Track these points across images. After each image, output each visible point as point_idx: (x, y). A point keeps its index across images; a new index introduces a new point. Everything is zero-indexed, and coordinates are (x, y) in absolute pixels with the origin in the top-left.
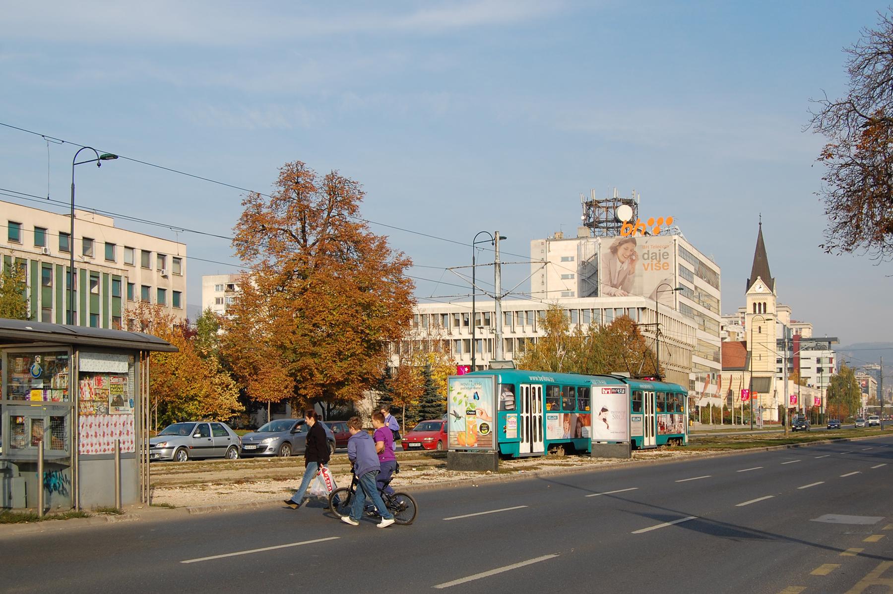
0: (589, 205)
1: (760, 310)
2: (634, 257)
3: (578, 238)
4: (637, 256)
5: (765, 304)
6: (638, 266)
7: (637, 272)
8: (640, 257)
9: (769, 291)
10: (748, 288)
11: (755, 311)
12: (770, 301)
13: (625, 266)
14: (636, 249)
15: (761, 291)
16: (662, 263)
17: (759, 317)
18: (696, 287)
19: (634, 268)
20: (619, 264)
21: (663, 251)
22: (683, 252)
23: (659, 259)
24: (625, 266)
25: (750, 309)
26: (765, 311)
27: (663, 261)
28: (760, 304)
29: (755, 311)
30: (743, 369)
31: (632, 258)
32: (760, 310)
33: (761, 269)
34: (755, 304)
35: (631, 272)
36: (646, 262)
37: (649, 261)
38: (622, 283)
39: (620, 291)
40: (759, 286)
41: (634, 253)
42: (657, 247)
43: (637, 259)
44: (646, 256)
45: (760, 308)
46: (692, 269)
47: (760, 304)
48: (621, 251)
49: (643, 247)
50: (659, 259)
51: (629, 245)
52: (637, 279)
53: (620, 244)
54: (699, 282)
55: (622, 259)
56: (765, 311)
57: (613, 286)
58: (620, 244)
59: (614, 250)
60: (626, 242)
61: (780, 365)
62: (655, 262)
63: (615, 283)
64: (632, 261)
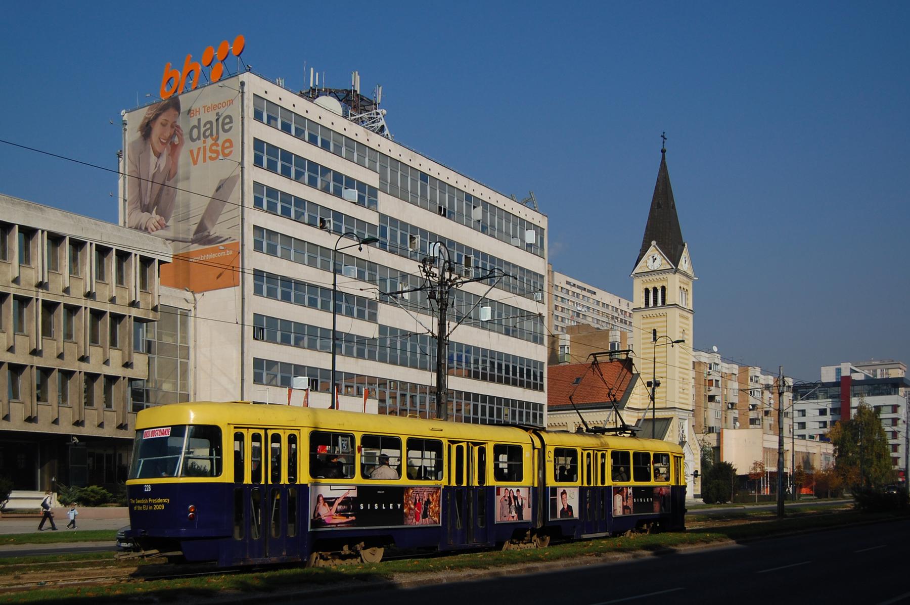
5: (663, 289)
6: (183, 157)
7: (180, 172)
8: (186, 137)
11: (647, 303)
14: (180, 122)
15: (656, 266)
16: (220, 142)
18: (383, 217)
19: (175, 164)
20: (153, 158)
27: (223, 137)
28: (655, 290)
29: (647, 303)
34: (647, 291)
35: (171, 173)
36: (195, 146)
37: (199, 143)
38: (157, 203)
39: (155, 217)
40: (654, 259)
41: (176, 130)
42: (215, 107)
44: (195, 131)
45: (656, 297)
46: (371, 179)
47: (655, 290)
48: (157, 130)
51: (171, 111)
53: (156, 117)
54: (389, 205)
55: (158, 149)
57: (146, 209)
60: (164, 109)
61: (823, 418)
62: (210, 141)
63: (147, 200)
64: (174, 148)
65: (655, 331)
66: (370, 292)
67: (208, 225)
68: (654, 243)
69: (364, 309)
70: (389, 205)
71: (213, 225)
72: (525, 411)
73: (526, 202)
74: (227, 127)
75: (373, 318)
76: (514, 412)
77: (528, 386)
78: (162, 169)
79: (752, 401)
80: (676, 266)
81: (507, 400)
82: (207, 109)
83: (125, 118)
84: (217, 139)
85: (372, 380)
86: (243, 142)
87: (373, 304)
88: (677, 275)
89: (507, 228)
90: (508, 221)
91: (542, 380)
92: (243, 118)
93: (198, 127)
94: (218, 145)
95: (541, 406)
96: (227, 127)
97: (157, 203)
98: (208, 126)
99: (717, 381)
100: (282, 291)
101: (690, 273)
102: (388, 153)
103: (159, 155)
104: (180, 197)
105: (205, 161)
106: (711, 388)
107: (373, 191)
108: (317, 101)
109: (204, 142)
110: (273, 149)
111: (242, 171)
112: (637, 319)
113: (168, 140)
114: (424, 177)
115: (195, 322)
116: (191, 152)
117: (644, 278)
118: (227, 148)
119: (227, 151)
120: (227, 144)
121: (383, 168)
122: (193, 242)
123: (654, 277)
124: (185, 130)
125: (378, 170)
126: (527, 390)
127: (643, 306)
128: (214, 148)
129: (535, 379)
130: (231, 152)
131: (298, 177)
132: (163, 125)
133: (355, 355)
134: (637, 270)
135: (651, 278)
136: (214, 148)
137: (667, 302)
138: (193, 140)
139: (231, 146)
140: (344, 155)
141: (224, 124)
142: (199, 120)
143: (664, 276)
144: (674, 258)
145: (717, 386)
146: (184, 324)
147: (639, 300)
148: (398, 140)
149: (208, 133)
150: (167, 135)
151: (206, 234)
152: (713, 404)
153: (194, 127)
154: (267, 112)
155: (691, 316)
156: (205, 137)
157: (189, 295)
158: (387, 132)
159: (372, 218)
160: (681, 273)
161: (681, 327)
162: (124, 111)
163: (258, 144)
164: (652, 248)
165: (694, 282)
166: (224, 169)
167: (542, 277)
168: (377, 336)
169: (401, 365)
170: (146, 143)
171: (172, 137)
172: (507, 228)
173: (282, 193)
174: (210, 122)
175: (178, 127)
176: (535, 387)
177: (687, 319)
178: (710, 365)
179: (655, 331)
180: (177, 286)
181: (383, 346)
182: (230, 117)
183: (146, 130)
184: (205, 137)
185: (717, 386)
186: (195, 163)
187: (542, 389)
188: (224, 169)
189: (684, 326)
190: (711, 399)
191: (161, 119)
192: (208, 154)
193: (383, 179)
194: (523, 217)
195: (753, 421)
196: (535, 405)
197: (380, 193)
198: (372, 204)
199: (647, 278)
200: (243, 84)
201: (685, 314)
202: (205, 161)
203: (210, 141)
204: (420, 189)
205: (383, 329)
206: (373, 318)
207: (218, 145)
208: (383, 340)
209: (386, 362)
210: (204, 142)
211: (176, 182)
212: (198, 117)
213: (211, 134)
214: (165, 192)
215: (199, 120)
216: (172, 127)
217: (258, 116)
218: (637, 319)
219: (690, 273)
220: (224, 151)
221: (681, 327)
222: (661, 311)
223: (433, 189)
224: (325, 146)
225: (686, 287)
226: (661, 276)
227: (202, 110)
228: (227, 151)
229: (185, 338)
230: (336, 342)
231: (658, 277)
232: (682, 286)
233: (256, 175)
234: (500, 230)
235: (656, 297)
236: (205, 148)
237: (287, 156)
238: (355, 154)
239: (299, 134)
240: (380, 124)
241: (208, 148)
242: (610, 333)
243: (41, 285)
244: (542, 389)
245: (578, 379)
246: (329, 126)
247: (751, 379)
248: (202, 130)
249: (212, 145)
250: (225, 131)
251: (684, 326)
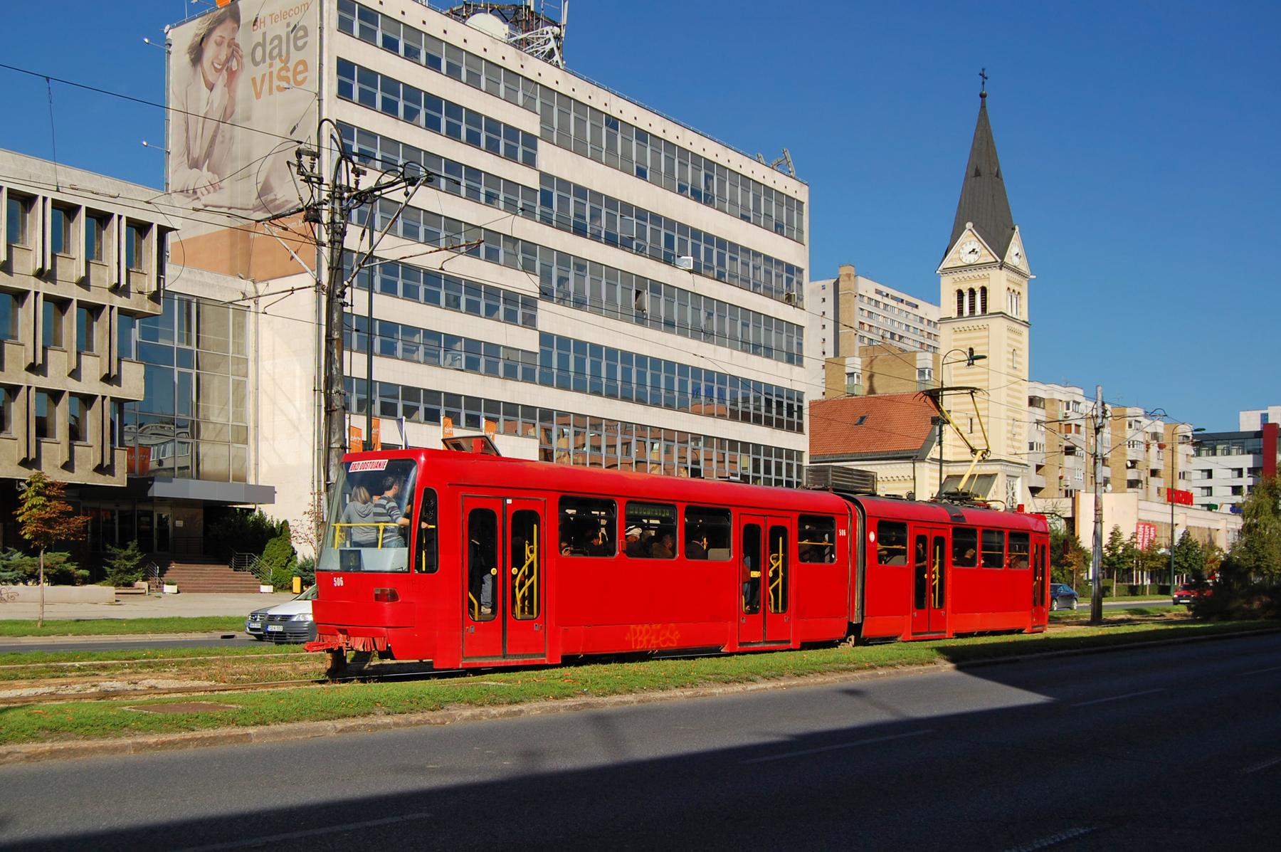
1: (972, 308)
5: (984, 290)
6: (243, 86)
7: (239, 109)
8: (247, 60)
11: (960, 312)
12: (998, 282)
14: (240, 39)
16: (291, 65)
17: (973, 323)
18: (545, 177)
19: (232, 99)
20: (205, 90)
26: (984, 309)
27: (295, 56)
28: (972, 292)
29: (960, 312)
30: (914, 457)
32: (972, 308)
34: (960, 293)
37: (263, 68)
38: (208, 155)
40: (969, 247)
42: (286, 14)
44: (259, 51)
45: (973, 302)
46: (529, 122)
47: (972, 292)
48: (210, 52)
51: (229, 24)
53: (209, 32)
56: (984, 309)
57: (195, 164)
58: (209, 32)
60: (219, 21)
63: (197, 152)
64: (232, 75)
65: (971, 349)
66: (526, 284)
68: (969, 225)
69: (517, 309)
70: (554, 160)
72: (784, 462)
73: (780, 167)
74: (300, 43)
75: (530, 322)
76: (756, 462)
77: (779, 425)
78: (215, 105)
79: (1131, 454)
80: (1002, 257)
81: (745, 445)
82: (274, 18)
83: (169, 36)
84: (287, 60)
85: (529, 411)
86: (321, 64)
87: (529, 303)
88: (1004, 272)
89: (745, 198)
90: (746, 191)
91: (800, 417)
92: (321, 29)
93: (263, 45)
94: (288, 70)
95: (800, 453)
96: (300, 43)
97: (208, 155)
98: (276, 42)
99: (1078, 426)
100: (383, 281)
101: (1024, 268)
102: (554, 87)
103: (211, 87)
104: (238, 148)
105: (271, 92)
106: (1069, 436)
107: (530, 140)
108: (471, 21)
109: (271, 65)
110: (368, 76)
111: (320, 106)
112: (945, 331)
113: (223, 65)
114: (613, 122)
115: (257, 324)
116: (254, 80)
117: (956, 276)
118: (301, 72)
119: (300, 78)
120: (301, 68)
121: (546, 108)
122: (255, 209)
123: (970, 274)
124: (245, 49)
125: (538, 109)
126: (778, 432)
127: (955, 315)
128: (283, 73)
129: (790, 414)
130: (305, 78)
131: (410, 116)
132: (219, 44)
133: (501, 373)
134: (947, 263)
135: (965, 275)
136: (283, 73)
137: (989, 311)
138: (256, 64)
139: (306, 70)
140: (483, 86)
141: (296, 39)
142: (264, 34)
143: (985, 272)
144: (1000, 248)
145: (1078, 432)
146: (241, 328)
147: (949, 305)
148: (573, 68)
149: (276, 52)
150: (223, 58)
151: (271, 197)
152: (1071, 457)
153: (258, 44)
155: (1025, 331)
156: (272, 58)
157: (248, 286)
158: (557, 58)
159: (529, 178)
160: (1009, 268)
161: (1009, 345)
162: (168, 27)
163: (345, 67)
164: (966, 233)
165: (1030, 281)
167: (800, 271)
168: (537, 349)
169: (576, 390)
170: (195, 71)
171: (228, 60)
172: (745, 198)
173: (383, 138)
174: (279, 37)
175: (237, 46)
176: (790, 427)
177: (1020, 334)
178: (1068, 404)
179: (971, 349)
180: (233, 272)
181: (546, 364)
182: (305, 29)
183: (197, 52)
184: (272, 58)
185: (1078, 432)
186: (258, 96)
187: (800, 429)
189: (1014, 343)
190: (1070, 451)
191: (216, 35)
192: (276, 83)
193: (545, 121)
194: (770, 184)
195: (1133, 484)
196: (790, 453)
197: (541, 145)
198: (530, 161)
199: (960, 275)
201: (1016, 326)
202: (271, 92)
203: (278, 64)
204: (609, 140)
205: (545, 338)
206: (530, 322)
207: (288, 70)
208: (546, 355)
209: (552, 386)
210: (271, 65)
212: (263, 29)
213: (280, 55)
214: (219, 138)
215: (264, 34)
216: (229, 46)
217: (345, 27)
218: (945, 331)
219: (1024, 268)
220: (292, 78)
221: (1009, 345)
222: (981, 323)
223: (626, 141)
224: (453, 72)
225: (1017, 289)
226: (980, 273)
227: (268, 21)
228: (300, 78)
229: (240, 347)
230: (478, 356)
231: (975, 273)
232: (1012, 287)
234: (733, 202)
235: (973, 302)
236: (271, 73)
237: (391, 84)
238: (502, 87)
239: (411, 54)
240: (548, 48)
241: (275, 75)
242: (919, 356)
243: (116, 289)
244: (800, 429)
245: (862, 419)
246: (461, 45)
247: (1130, 426)
248: (268, 48)
249: (282, 69)
250: (298, 49)
251: (1014, 343)
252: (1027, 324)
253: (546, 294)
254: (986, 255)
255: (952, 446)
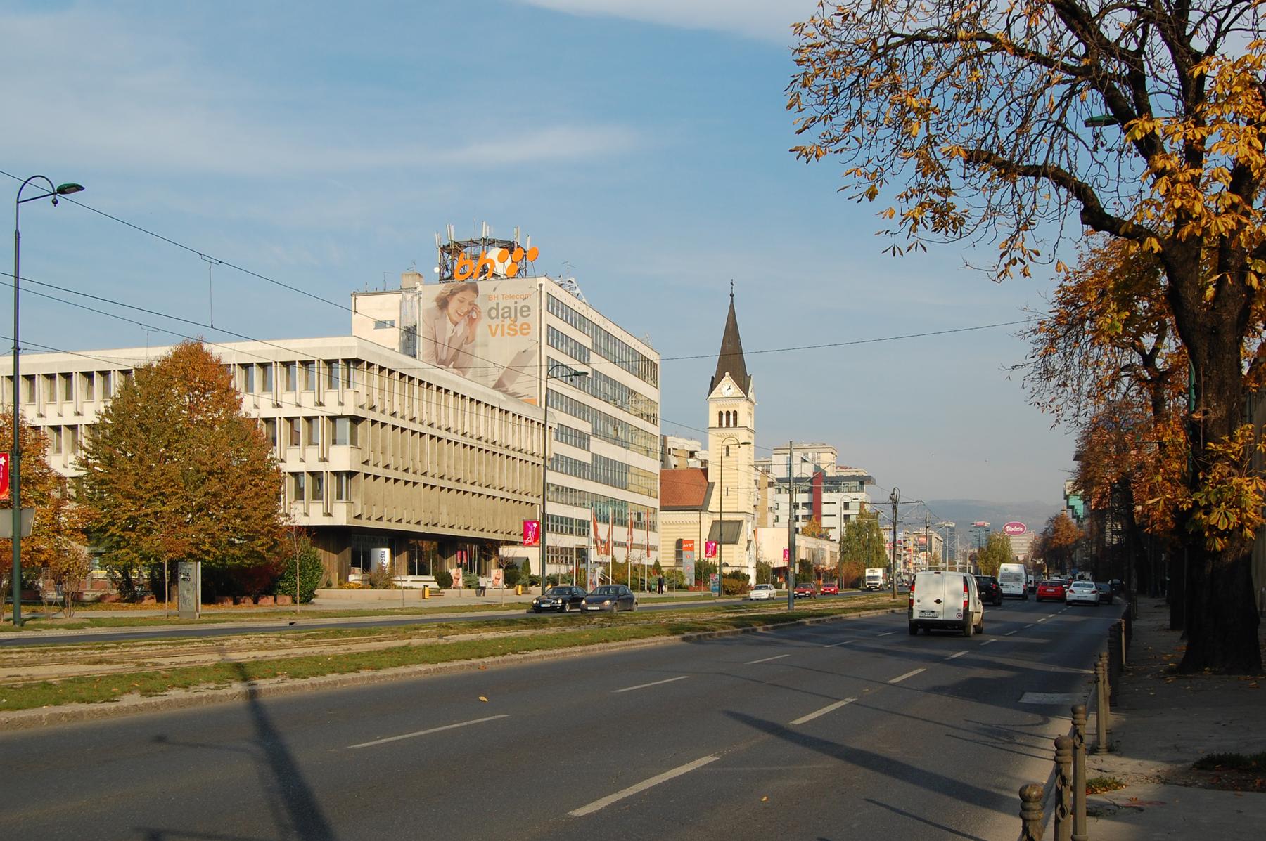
0: (453, 249)
1: (728, 422)
2: (474, 315)
3: (400, 291)
4: (479, 313)
5: (735, 413)
6: (481, 328)
7: (479, 339)
9: (741, 394)
10: (712, 388)
11: (721, 424)
12: (743, 408)
13: (460, 329)
14: (478, 301)
15: (729, 393)
16: (518, 323)
19: (473, 333)
20: (450, 326)
21: (521, 303)
22: (555, 306)
23: (515, 315)
24: (460, 329)
25: (714, 421)
26: (735, 424)
27: (521, 320)
29: (721, 424)
31: (471, 317)
32: (728, 422)
33: (732, 361)
34: (721, 413)
35: (470, 339)
36: (494, 323)
37: (499, 321)
38: (454, 359)
40: (727, 386)
41: (474, 307)
42: (513, 297)
43: (479, 317)
44: (493, 313)
45: (728, 419)
47: (728, 413)
48: (453, 304)
49: (490, 298)
50: (515, 315)
52: (479, 352)
53: (453, 293)
55: (455, 318)
56: (735, 424)
58: (453, 293)
59: (443, 303)
60: (463, 289)
62: (508, 321)
63: (444, 357)
64: (472, 321)
67: (507, 383)
71: (512, 382)
80: (746, 392)
97: (454, 359)
103: (456, 324)
141: (521, 311)
154: (555, 306)
166: (520, 343)
171: (469, 312)
186: (493, 335)
188: (520, 343)
191: (459, 296)
192: (507, 331)
200: (541, 285)
211: (474, 347)
213: (510, 316)
233: (548, 351)
252: (754, 432)
253: (595, 433)
254: (735, 391)
255: (714, 505)
